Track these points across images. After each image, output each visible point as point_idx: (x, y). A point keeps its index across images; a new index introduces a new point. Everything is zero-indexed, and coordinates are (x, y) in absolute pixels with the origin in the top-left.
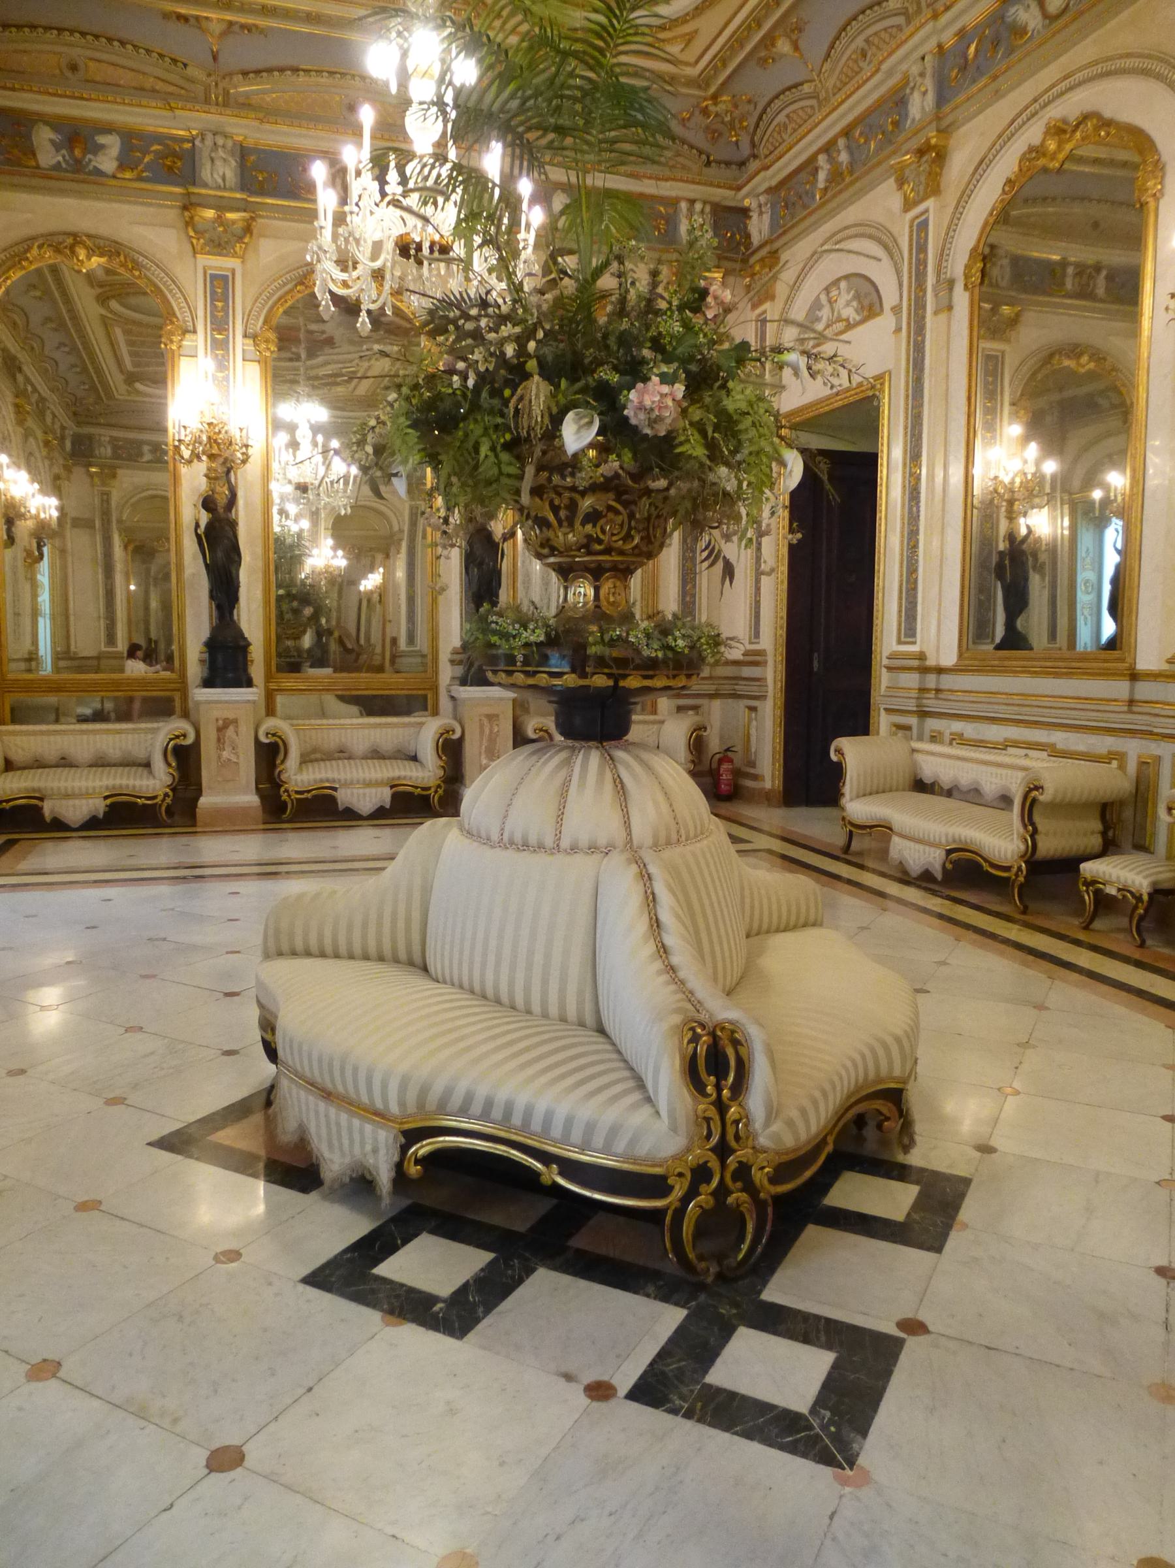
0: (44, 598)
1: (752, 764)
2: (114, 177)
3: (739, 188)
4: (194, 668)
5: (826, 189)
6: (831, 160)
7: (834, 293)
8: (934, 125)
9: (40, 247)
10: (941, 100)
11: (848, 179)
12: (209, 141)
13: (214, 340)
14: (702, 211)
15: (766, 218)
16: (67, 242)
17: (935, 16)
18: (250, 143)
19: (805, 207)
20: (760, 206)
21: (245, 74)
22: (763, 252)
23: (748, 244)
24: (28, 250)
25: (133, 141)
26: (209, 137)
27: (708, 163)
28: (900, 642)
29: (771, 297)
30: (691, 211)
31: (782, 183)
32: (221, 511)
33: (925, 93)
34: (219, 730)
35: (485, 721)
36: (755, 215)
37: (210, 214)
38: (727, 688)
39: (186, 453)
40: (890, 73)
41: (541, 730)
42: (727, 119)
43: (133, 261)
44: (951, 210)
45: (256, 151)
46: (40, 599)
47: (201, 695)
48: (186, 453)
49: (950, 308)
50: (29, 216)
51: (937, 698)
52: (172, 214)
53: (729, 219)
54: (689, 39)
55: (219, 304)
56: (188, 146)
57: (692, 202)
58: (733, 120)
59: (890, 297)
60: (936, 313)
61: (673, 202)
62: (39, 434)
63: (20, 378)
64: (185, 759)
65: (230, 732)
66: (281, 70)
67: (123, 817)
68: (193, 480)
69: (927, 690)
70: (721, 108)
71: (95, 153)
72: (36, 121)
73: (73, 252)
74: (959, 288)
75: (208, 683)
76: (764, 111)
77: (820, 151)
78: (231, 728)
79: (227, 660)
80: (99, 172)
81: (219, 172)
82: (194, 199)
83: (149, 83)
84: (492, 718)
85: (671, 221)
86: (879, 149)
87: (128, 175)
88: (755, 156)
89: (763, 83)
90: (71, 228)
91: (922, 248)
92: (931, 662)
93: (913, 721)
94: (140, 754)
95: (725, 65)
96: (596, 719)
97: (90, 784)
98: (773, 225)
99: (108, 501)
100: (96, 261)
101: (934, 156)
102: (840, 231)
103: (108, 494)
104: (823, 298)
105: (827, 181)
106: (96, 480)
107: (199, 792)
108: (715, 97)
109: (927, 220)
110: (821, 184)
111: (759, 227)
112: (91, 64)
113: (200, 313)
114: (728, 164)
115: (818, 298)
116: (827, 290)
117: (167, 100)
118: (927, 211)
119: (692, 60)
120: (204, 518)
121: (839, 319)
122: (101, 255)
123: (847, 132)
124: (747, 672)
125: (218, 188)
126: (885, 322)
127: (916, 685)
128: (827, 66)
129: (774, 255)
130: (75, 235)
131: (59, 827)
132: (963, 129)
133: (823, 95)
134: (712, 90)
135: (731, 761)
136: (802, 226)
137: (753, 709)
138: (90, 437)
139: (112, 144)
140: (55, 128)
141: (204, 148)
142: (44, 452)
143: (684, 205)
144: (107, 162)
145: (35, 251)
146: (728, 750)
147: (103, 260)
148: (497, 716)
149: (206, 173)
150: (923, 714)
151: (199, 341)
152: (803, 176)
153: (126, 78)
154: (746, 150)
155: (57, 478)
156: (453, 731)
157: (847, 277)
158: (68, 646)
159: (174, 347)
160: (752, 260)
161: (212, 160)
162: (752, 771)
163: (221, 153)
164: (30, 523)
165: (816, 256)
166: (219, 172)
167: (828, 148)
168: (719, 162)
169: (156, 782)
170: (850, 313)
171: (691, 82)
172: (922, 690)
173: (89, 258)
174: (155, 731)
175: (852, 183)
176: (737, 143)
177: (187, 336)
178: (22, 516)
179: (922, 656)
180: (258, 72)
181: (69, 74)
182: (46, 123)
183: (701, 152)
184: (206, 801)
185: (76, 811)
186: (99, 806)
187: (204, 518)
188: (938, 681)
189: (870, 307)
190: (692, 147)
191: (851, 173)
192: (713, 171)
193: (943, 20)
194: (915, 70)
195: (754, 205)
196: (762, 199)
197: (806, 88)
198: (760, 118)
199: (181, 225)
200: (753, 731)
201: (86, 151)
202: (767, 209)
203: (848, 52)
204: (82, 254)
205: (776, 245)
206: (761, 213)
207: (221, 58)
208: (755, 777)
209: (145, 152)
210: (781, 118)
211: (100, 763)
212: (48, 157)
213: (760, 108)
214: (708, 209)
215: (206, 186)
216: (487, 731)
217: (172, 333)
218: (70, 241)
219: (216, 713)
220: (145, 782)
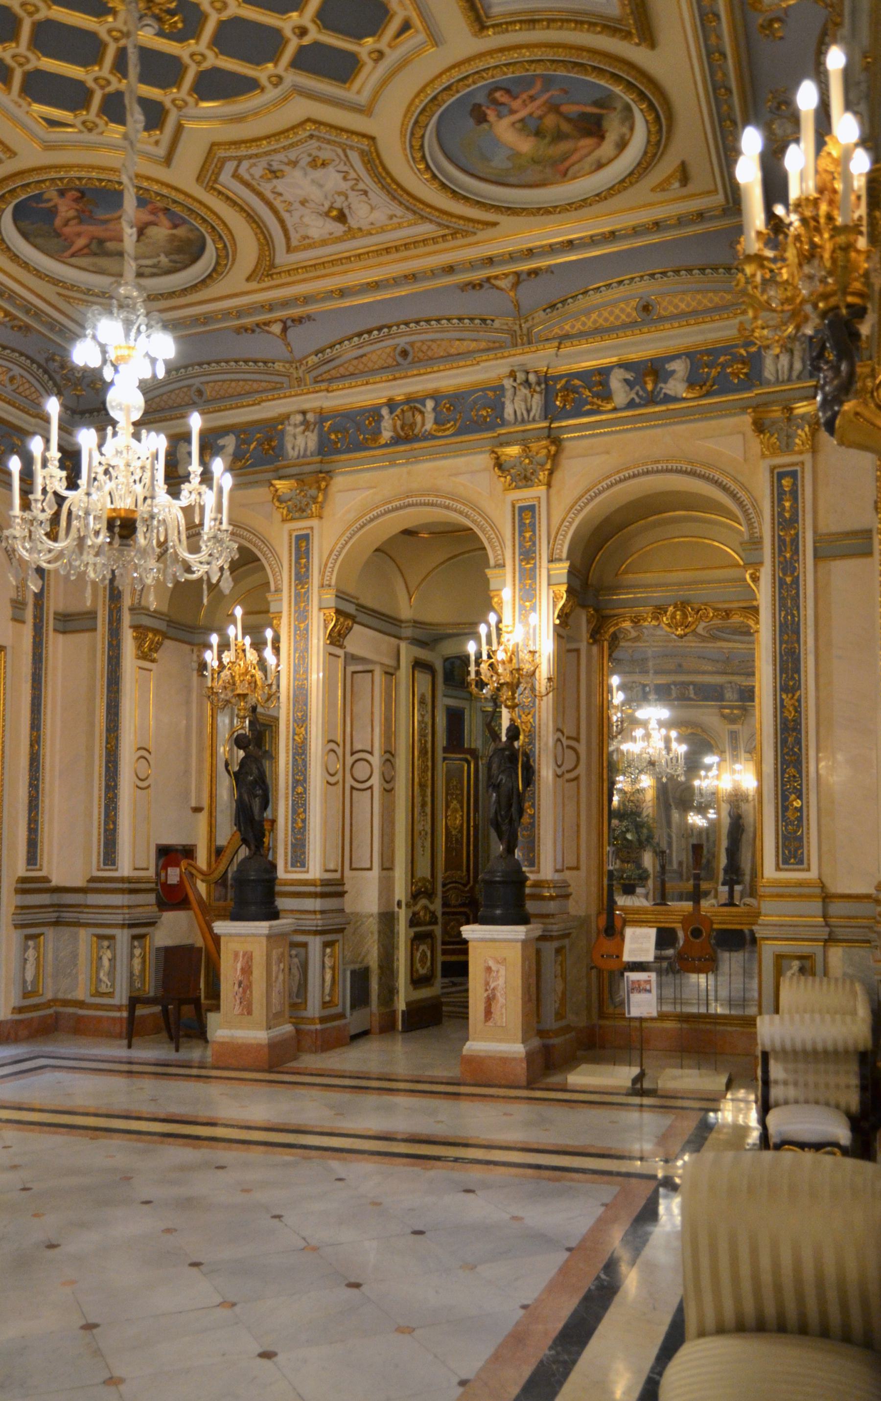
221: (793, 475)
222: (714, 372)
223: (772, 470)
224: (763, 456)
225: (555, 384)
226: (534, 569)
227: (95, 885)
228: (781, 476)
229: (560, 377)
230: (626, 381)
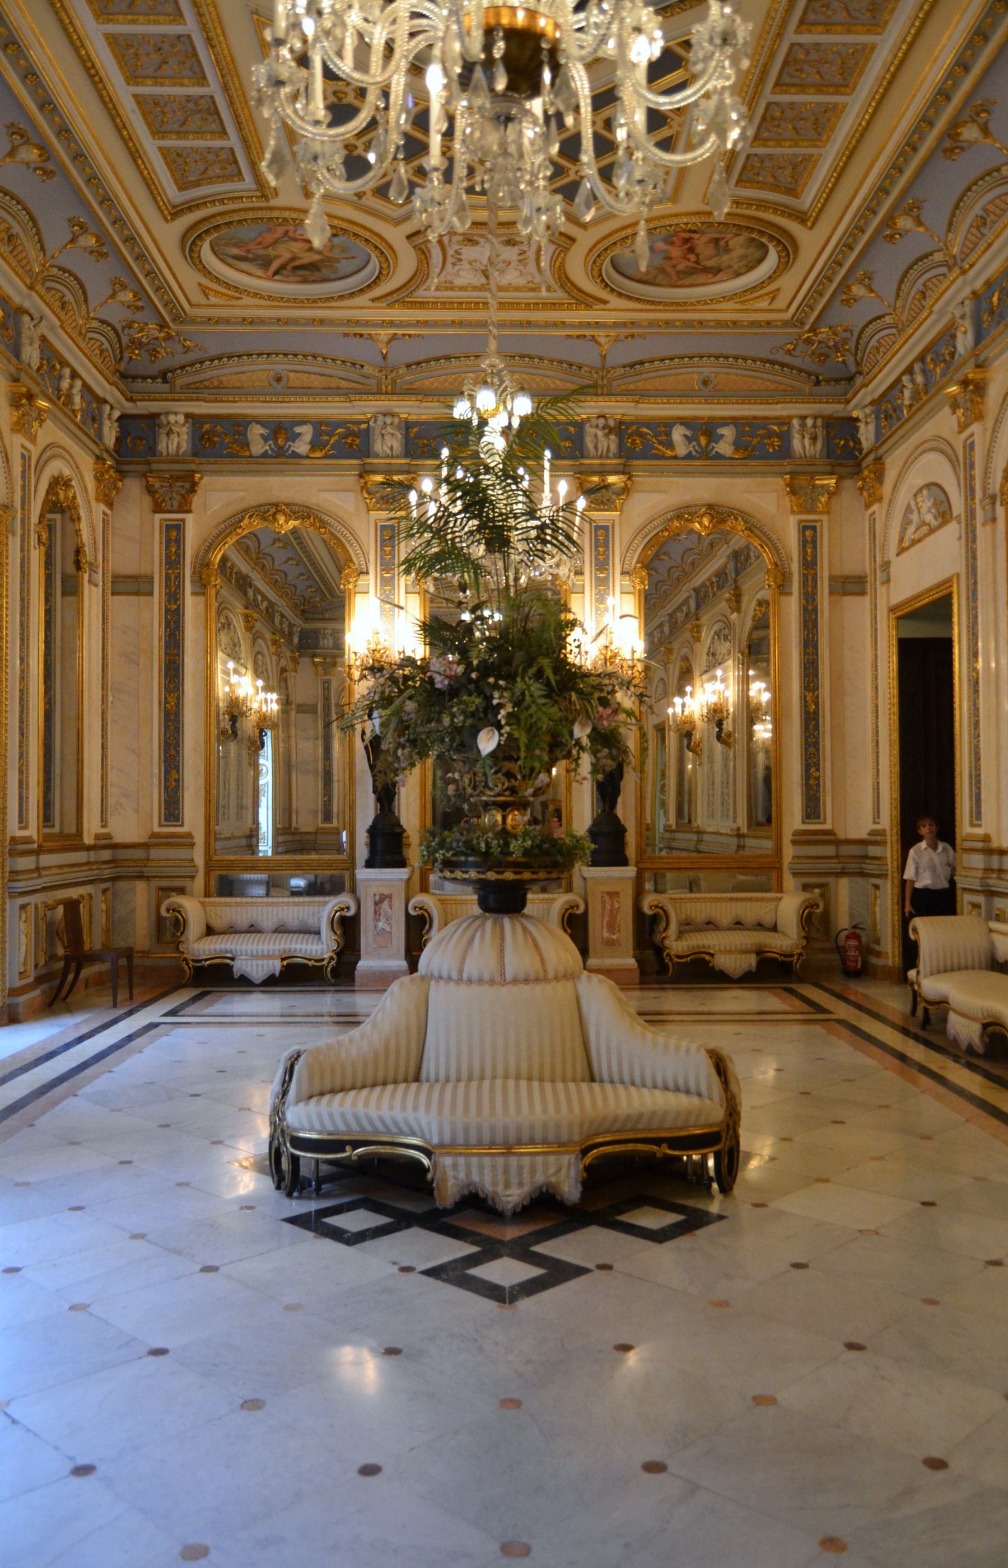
0: (266, 780)
1: (877, 941)
2: (307, 457)
3: (848, 402)
4: (362, 852)
5: (911, 406)
6: (913, 381)
7: (919, 499)
8: (972, 363)
9: (250, 517)
10: (979, 337)
11: (924, 398)
12: (380, 423)
13: (382, 578)
14: (814, 426)
15: (871, 427)
16: (269, 510)
17: (964, 272)
18: (413, 418)
19: (899, 419)
20: (866, 416)
21: (408, 366)
22: (871, 457)
23: (861, 450)
24: (241, 521)
25: (322, 428)
26: (380, 418)
27: (818, 383)
28: (972, 825)
29: (880, 500)
30: (803, 425)
31: (883, 395)
33: (965, 333)
34: (376, 904)
35: (607, 898)
36: (862, 426)
37: (379, 478)
38: (853, 867)
39: (356, 674)
40: (941, 314)
41: (656, 907)
42: (831, 343)
43: (321, 521)
44: (989, 433)
45: (416, 424)
46: (261, 782)
47: (363, 874)
48: (356, 674)
49: (994, 520)
50: (243, 493)
51: (999, 878)
52: (351, 480)
53: (840, 432)
54: (774, 295)
55: (388, 549)
56: (364, 426)
57: (803, 418)
58: (836, 346)
59: (958, 506)
60: (984, 524)
61: (785, 421)
62: (268, 636)
63: (250, 593)
64: (348, 928)
65: (385, 905)
66: (437, 359)
67: (295, 976)
69: (992, 870)
70: (820, 337)
71: (293, 441)
72: (250, 422)
73: (275, 520)
74: (998, 503)
75: (369, 864)
76: (859, 337)
77: (903, 373)
78: (386, 902)
79: (387, 845)
80: (295, 455)
81: (388, 444)
82: (367, 468)
83: (334, 382)
84: (613, 895)
85: (785, 438)
86: (943, 375)
87: (318, 454)
88: (860, 373)
89: (855, 317)
90: (273, 499)
91: (972, 466)
92: (995, 844)
93: (981, 899)
94: (312, 922)
95: (812, 309)
96: (503, 901)
97: (271, 947)
98: (878, 433)
99: (329, 689)
100: (292, 524)
101: (976, 388)
102: (921, 444)
103: (328, 682)
104: (913, 503)
105: (912, 398)
106: (320, 669)
108: (813, 329)
109: (972, 445)
110: (907, 402)
111: (866, 435)
112: (292, 375)
113: (372, 558)
114: (837, 381)
115: (909, 505)
116: (915, 495)
117: (348, 394)
118: (972, 435)
119: (784, 306)
121: (924, 524)
122: (296, 519)
123: (921, 358)
124: (873, 851)
125: (387, 457)
126: (952, 531)
127: (982, 866)
128: (899, 303)
129: (879, 459)
130: (276, 505)
131: (244, 984)
132: (996, 363)
133: (900, 326)
134: (807, 327)
135: (858, 937)
136: (896, 437)
137: (877, 887)
138: (316, 632)
139: (306, 432)
140: (263, 424)
141: (376, 426)
142: (273, 649)
143: (795, 422)
144: (302, 447)
145: (246, 521)
146: (855, 927)
147: (297, 523)
148: (617, 894)
149: (378, 446)
150: (990, 894)
151: (370, 581)
152: (896, 392)
153: (317, 382)
154: (853, 369)
155: (283, 670)
156: (577, 907)
157: (928, 486)
158: (290, 825)
159: (351, 586)
160: (864, 464)
161: (383, 435)
162: (877, 947)
163: (389, 429)
164: (253, 718)
165: (907, 464)
166: (388, 444)
167: (909, 370)
168: (828, 381)
169: (321, 948)
170: (929, 518)
171: (785, 324)
172: (988, 870)
173: (287, 522)
174: (325, 903)
175: (928, 401)
176: (844, 362)
177: (362, 577)
178: (243, 714)
179: (986, 838)
180: (418, 363)
181: (274, 384)
182: (258, 422)
183: (809, 374)
184: (362, 965)
185: (258, 970)
186: (276, 966)
188: (1001, 863)
189: (945, 516)
190: (800, 370)
191: (926, 393)
192: (824, 388)
193: (972, 273)
194: (958, 313)
195: (861, 416)
196: (868, 410)
197: (888, 319)
198: (858, 343)
199: (359, 488)
200: (877, 909)
201: (287, 440)
202: (872, 419)
203: (913, 293)
204: (281, 519)
205: (881, 452)
206: (867, 423)
207: (389, 357)
208: (878, 954)
209: (331, 436)
210: (873, 343)
211: (281, 930)
212: (258, 447)
213: (856, 334)
214: (819, 422)
215: (377, 456)
216: (608, 907)
217: (348, 576)
218: (273, 510)
219: (374, 890)
220: (314, 947)
221: (814, 529)
222: (755, 441)
223: (800, 522)
224: (793, 512)
225: (627, 428)
226: (607, 578)
227: (155, 842)
228: (805, 528)
229: (632, 423)
230: (685, 436)
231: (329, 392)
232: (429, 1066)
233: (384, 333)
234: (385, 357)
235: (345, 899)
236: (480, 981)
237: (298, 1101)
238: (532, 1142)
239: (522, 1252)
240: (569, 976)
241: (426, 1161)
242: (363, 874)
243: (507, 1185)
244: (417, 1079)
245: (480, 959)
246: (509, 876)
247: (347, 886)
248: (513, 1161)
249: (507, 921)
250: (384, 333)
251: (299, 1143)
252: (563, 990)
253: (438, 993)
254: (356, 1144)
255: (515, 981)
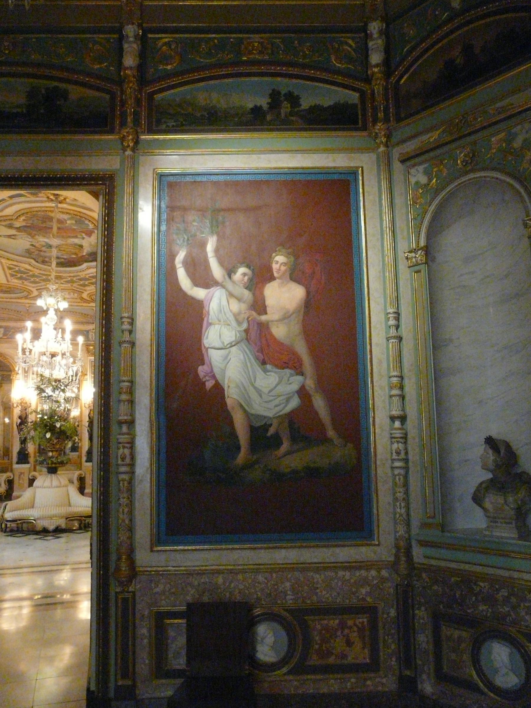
4: (15, 459)
13: (25, 376)
21: (35, 313)
32: (23, 418)
39: (15, 405)
43: (5, 357)
47: (15, 466)
64: (10, 483)
65: (22, 476)
68: (17, 412)
79: (23, 457)
87: (5, 337)
96: (53, 471)
107: (13, 492)
120: (19, 421)
174: (2, 476)
184: (14, 494)
187: (19, 421)
231: (10, 319)
232: (36, 505)
233: (28, 305)
234: (28, 310)
235: (9, 474)
236: (47, 487)
237: (8, 512)
238: (56, 517)
239: (52, 536)
240: (66, 486)
241: (34, 522)
242: (15, 466)
243: (51, 525)
244: (33, 507)
245: (47, 483)
246: (54, 465)
247: (10, 470)
248: (52, 521)
249: (53, 475)
250: (28, 305)
251: (8, 521)
252: (65, 489)
253: (38, 491)
254: (20, 520)
255: (54, 487)
